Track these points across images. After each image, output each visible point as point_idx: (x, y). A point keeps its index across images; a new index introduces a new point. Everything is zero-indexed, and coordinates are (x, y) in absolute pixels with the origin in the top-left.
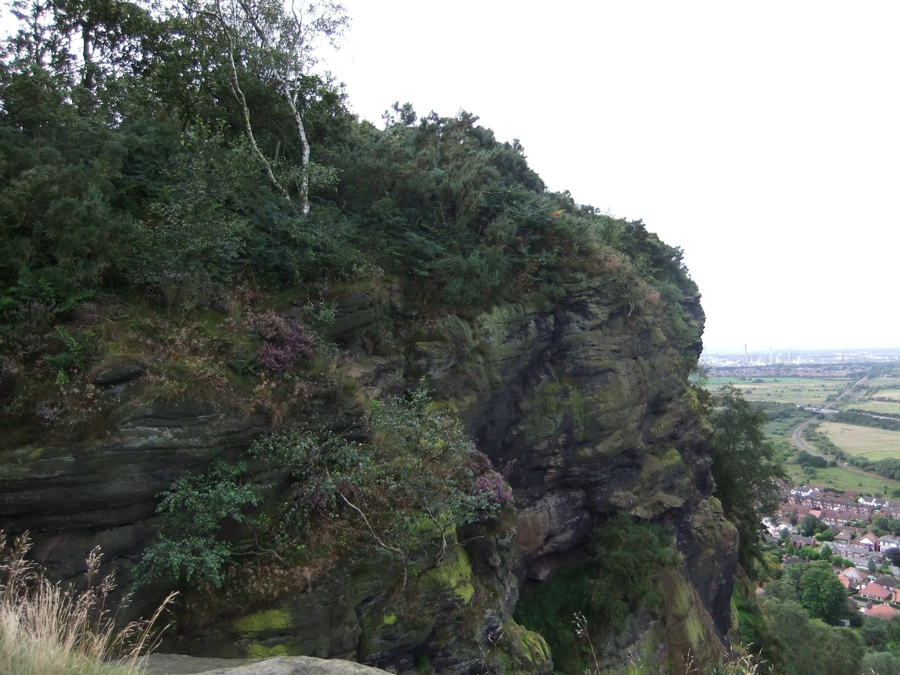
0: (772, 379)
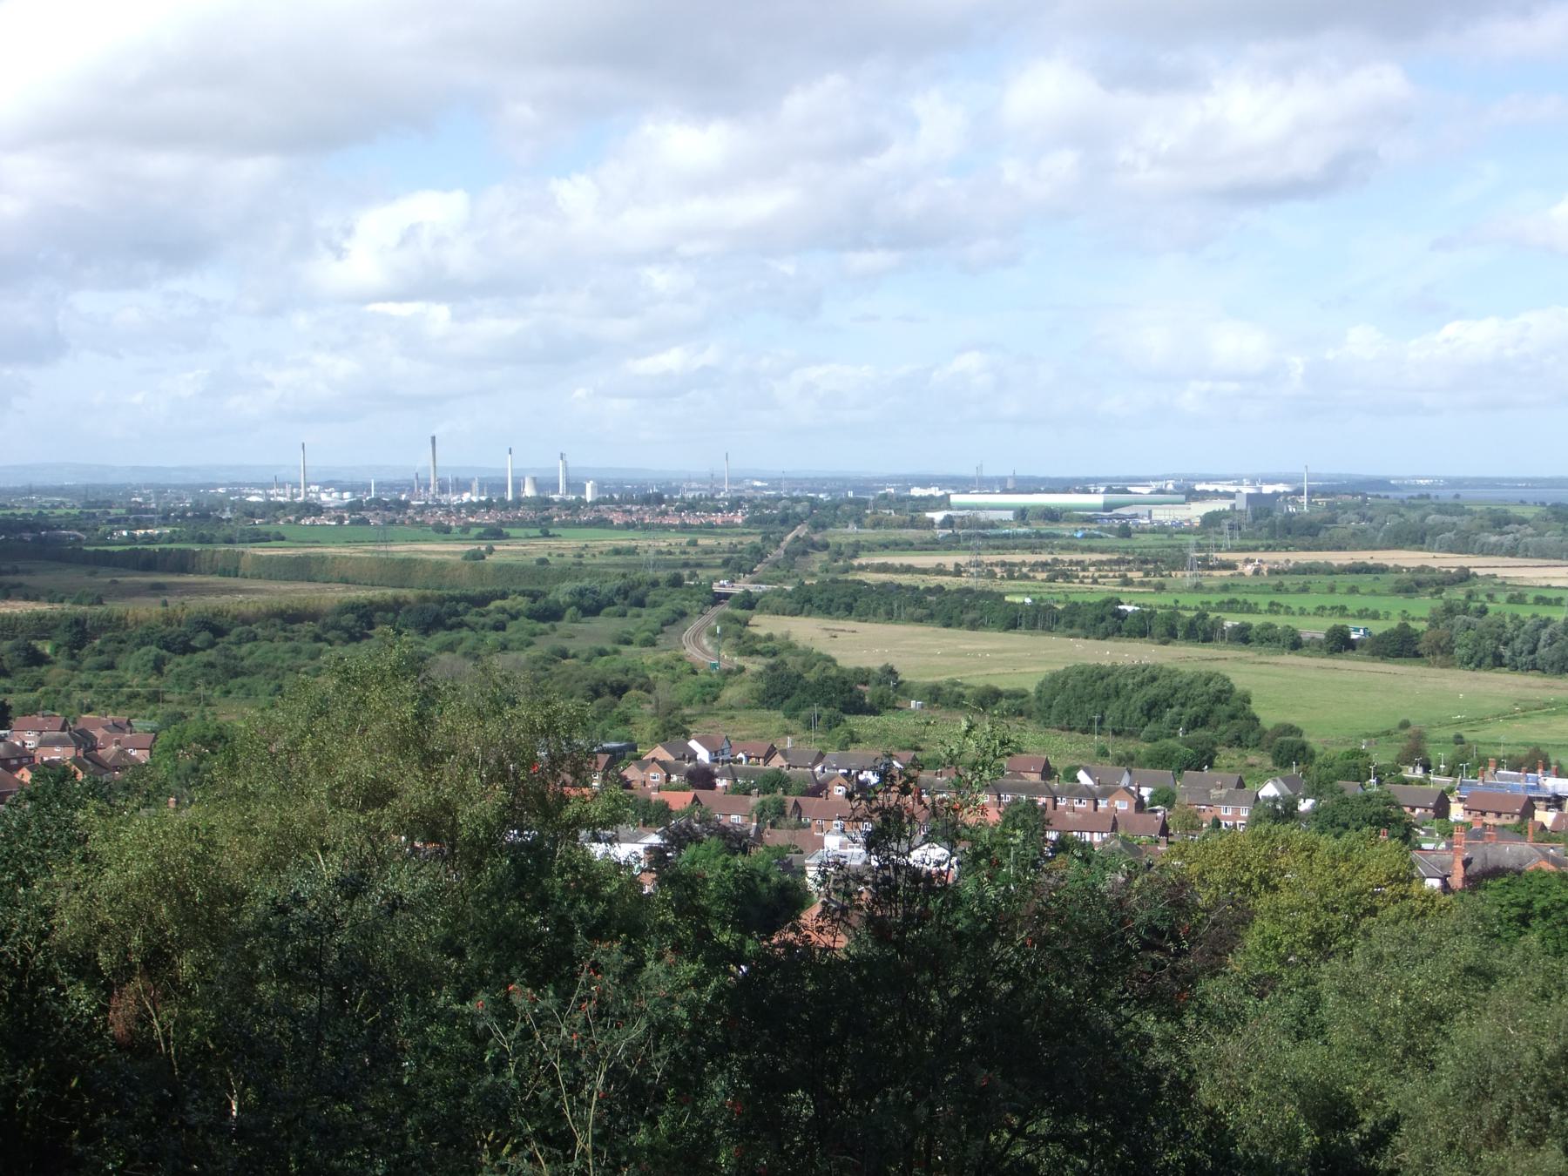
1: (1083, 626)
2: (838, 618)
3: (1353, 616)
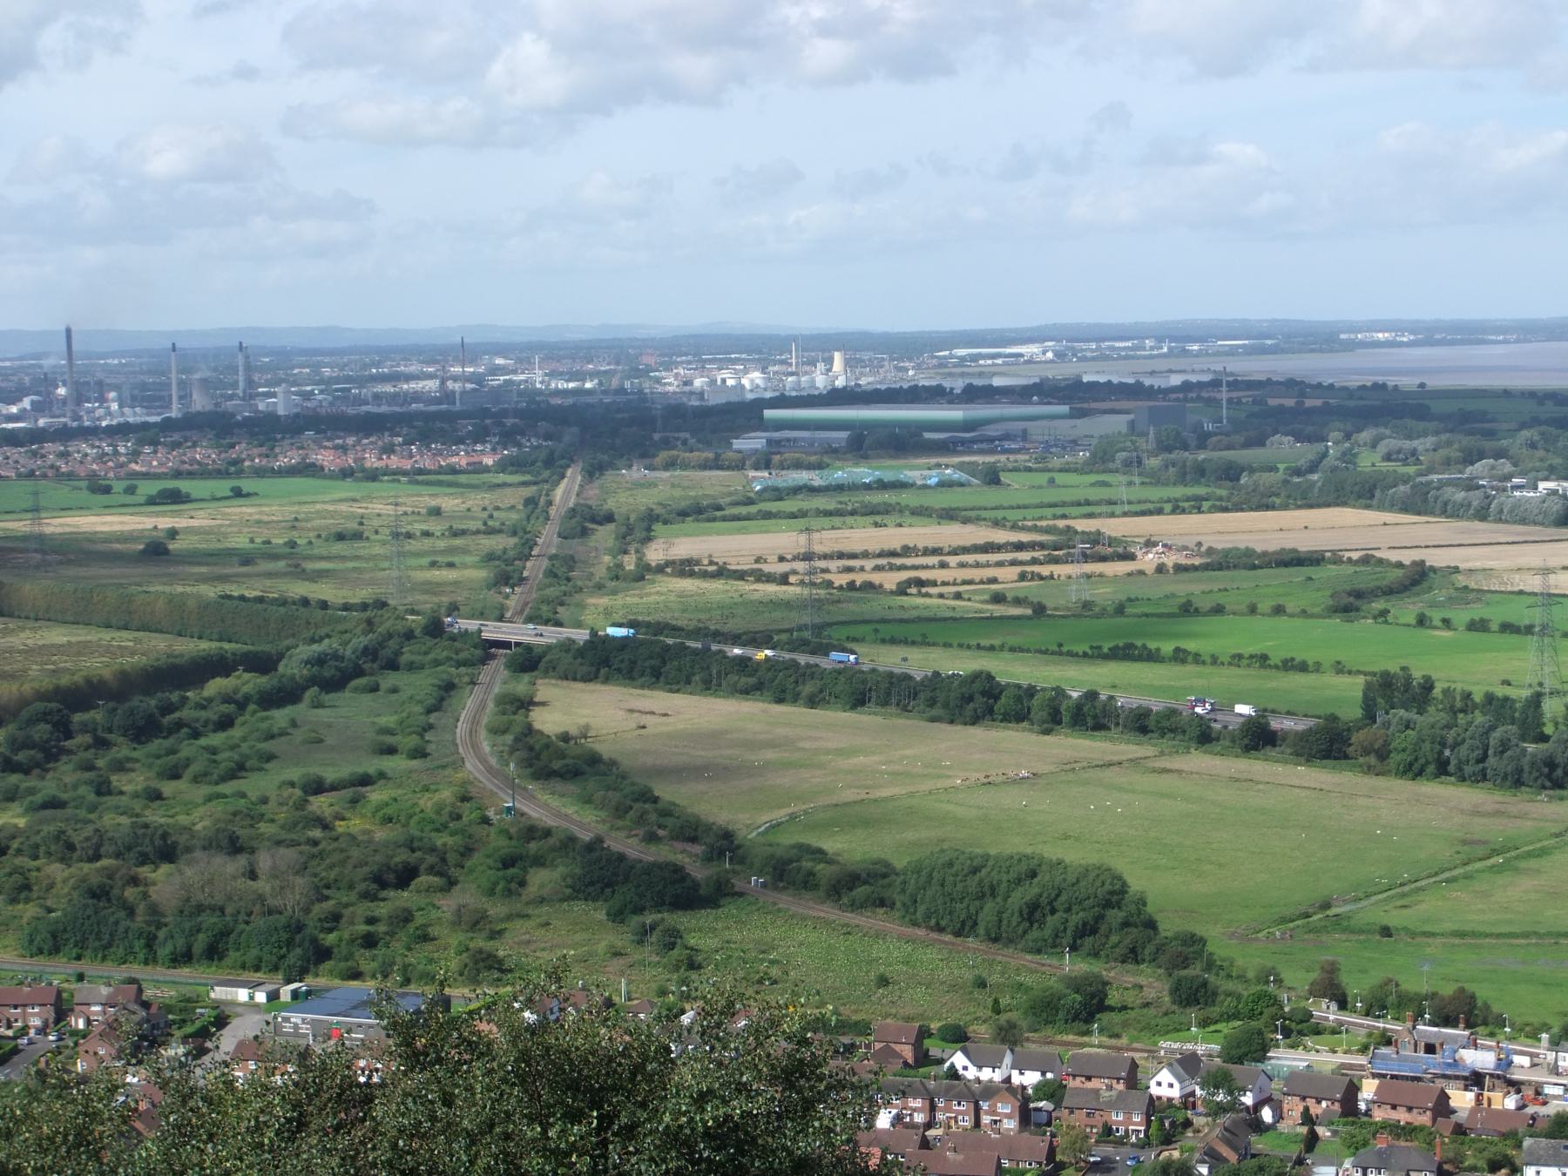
0: (223, 486)
1: (946, 706)
2: (642, 687)
3: (1276, 667)
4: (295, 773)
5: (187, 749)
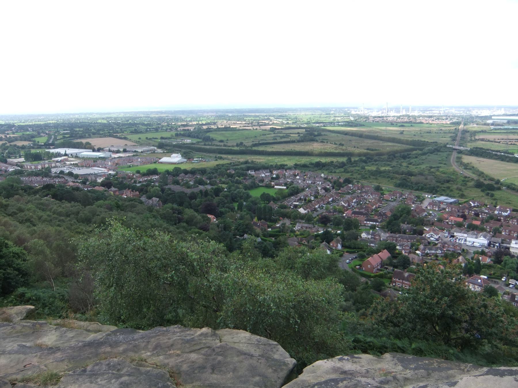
0: (410, 125)
4: (428, 165)
5: (412, 161)
